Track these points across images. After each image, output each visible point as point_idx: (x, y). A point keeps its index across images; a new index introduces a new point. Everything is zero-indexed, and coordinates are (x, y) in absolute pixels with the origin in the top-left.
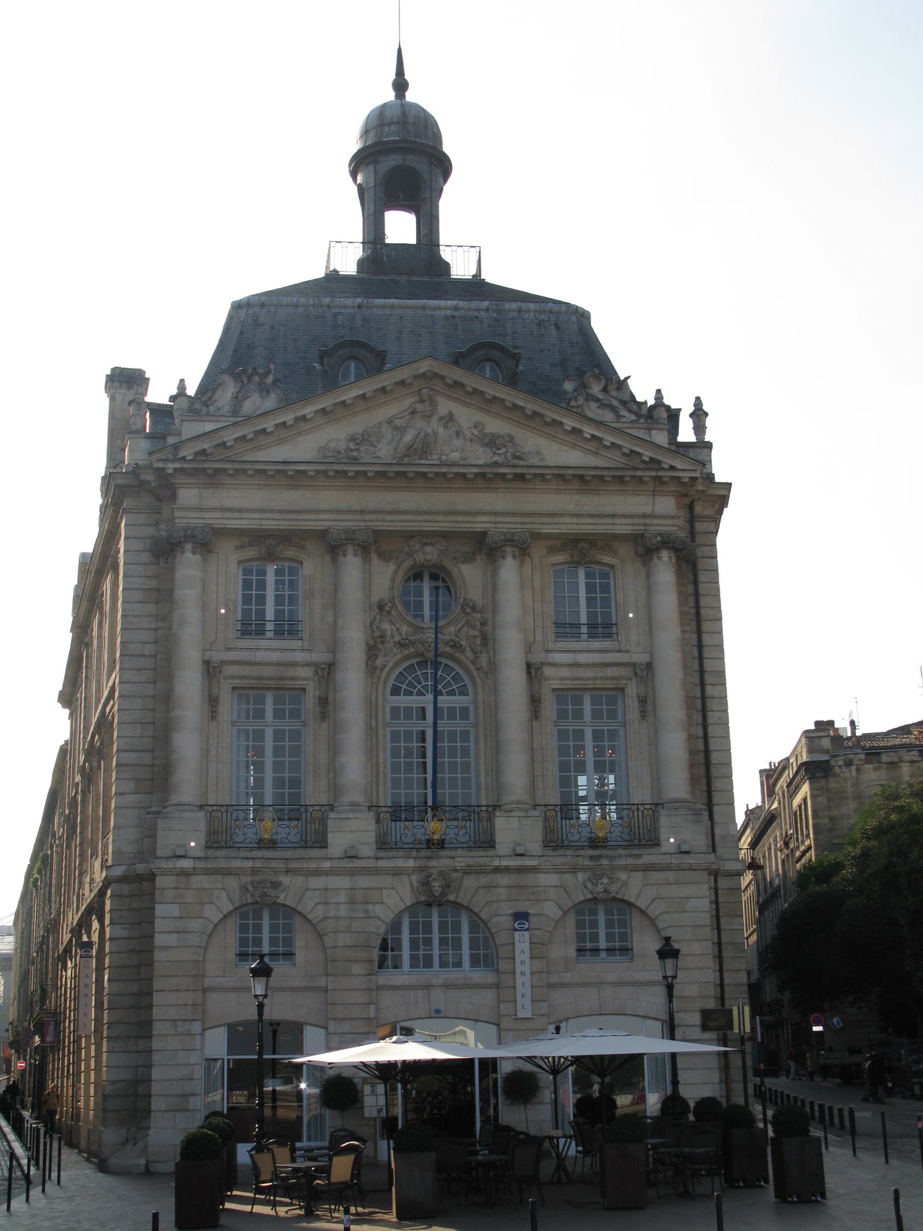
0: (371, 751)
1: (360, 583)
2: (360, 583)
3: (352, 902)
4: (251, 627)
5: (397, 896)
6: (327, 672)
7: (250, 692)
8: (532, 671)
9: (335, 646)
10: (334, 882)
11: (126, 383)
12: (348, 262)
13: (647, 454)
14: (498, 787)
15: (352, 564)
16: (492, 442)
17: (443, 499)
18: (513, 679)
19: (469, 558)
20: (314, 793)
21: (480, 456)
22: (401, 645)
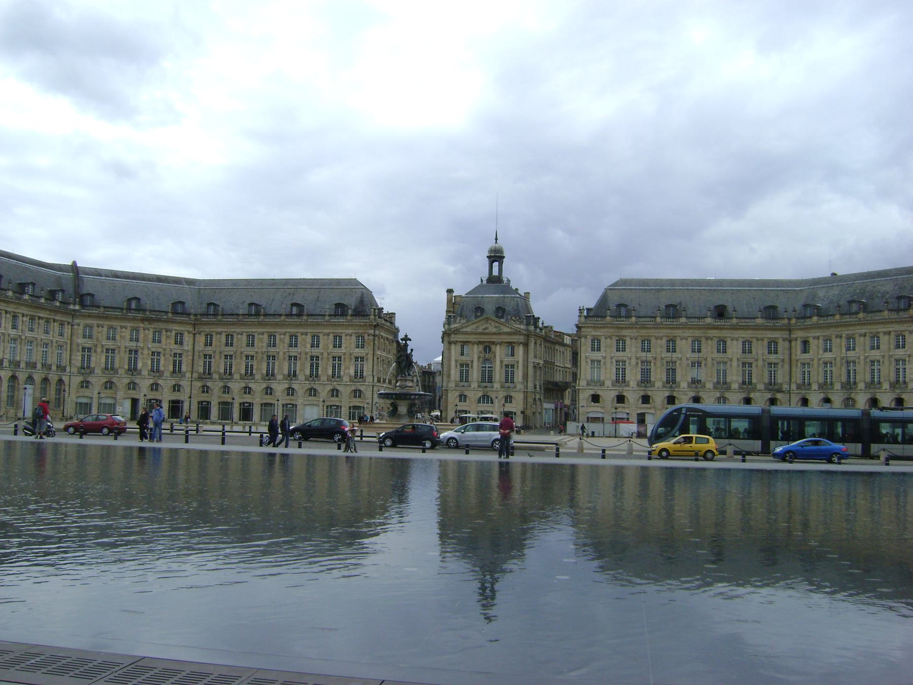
5: (481, 394)
7: (462, 365)
8: (501, 362)
11: (450, 291)
15: (476, 346)
18: (498, 363)
21: (494, 330)
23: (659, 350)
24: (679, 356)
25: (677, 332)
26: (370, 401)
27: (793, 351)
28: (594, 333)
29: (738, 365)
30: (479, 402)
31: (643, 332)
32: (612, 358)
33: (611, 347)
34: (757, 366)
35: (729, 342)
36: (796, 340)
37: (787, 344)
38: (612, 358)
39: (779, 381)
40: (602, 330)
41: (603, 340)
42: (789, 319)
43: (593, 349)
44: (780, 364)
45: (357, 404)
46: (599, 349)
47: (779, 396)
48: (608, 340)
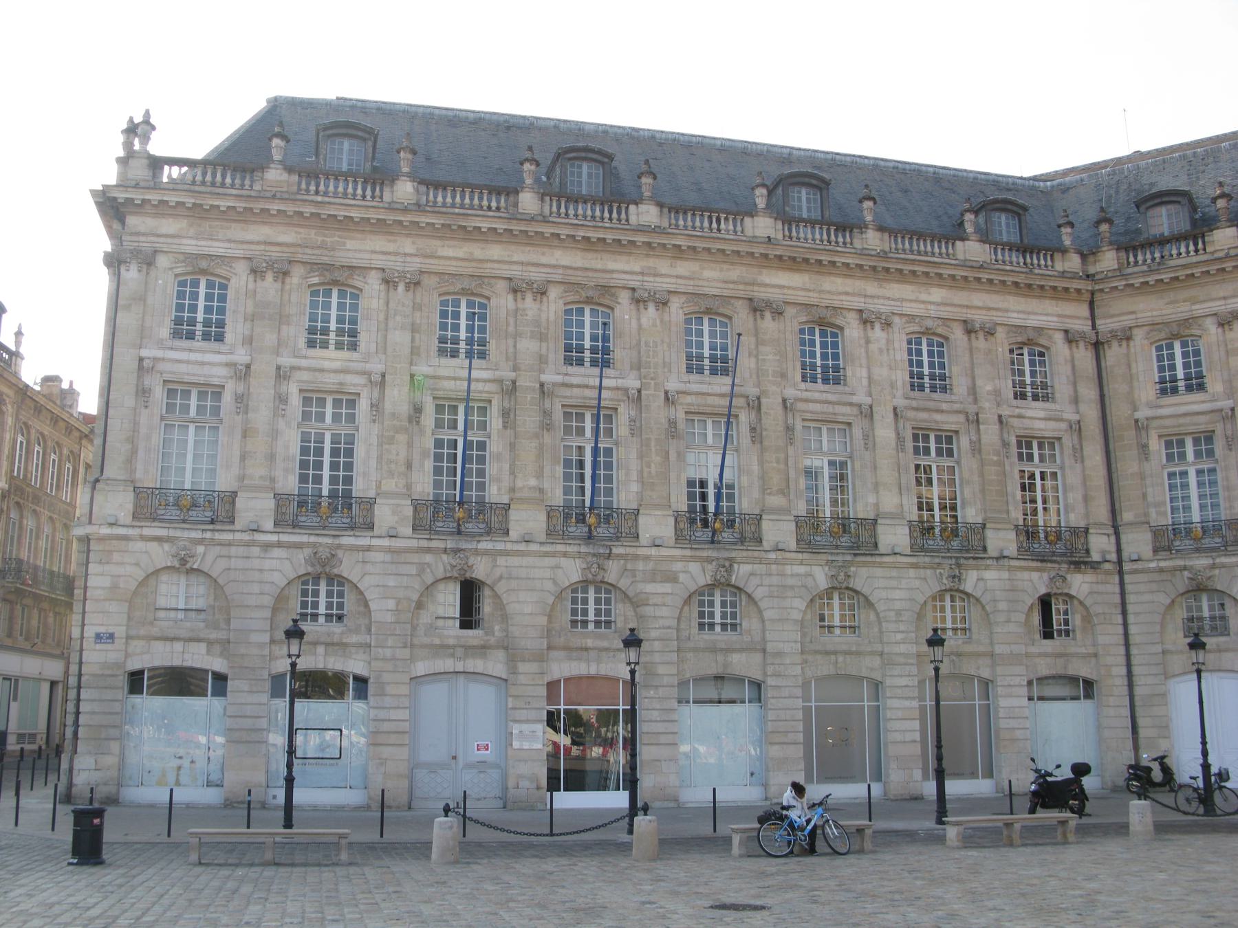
23: (528, 346)
24: (632, 383)
25: (622, 268)
27: (1116, 388)
28: (191, 245)
29: (900, 439)
31: (453, 254)
32: (281, 375)
33: (282, 319)
34: (976, 448)
35: (853, 331)
36: (1126, 336)
37: (1084, 356)
39: (1075, 519)
40: (238, 232)
41: (240, 280)
42: (1088, 254)
43: (183, 330)
44: (1068, 442)
46: (215, 333)
47: (1080, 584)
48: (269, 284)
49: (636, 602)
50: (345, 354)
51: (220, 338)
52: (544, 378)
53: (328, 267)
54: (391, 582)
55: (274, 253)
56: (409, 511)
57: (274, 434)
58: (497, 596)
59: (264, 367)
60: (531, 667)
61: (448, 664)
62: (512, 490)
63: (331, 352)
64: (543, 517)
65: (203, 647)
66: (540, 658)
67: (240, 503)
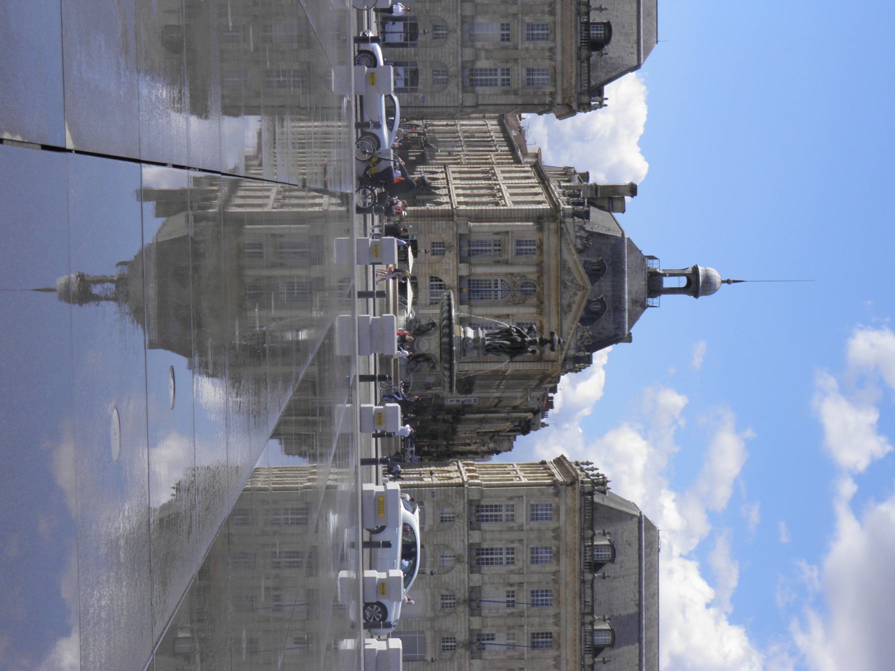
0: (486, 274)
1: (530, 271)
2: (530, 271)
3: (446, 270)
4: (519, 243)
6: (506, 263)
7: (498, 244)
9: (513, 264)
10: (451, 266)
11: (633, 190)
12: (653, 265)
13: (566, 347)
14: (476, 306)
16: (569, 306)
17: (553, 293)
18: (505, 311)
19: (538, 300)
20: (474, 260)
22: (514, 282)
23: (536, 620)
26: (429, 102)
28: (563, 509)
30: (432, 279)
32: (521, 541)
33: (540, 539)
38: (521, 541)
41: (552, 525)
43: (533, 507)
45: (421, 78)
46: (534, 518)
49: (451, 659)
50: (529, 559)
51: (532, 519)
52: (525, 627)
53: (558, 552)
54: (454, 581)
55: (563, 535)
56: (477, 585)
57: (501, 540)
58: (451, 613)
59: (523, 535)
60: (429, 626)
61: (429, 599)
62: (487, 617)
63: (529, 555)
64: (478, 627)
65: (431, 523)
66: (432, 628)
67: (477, 531)
